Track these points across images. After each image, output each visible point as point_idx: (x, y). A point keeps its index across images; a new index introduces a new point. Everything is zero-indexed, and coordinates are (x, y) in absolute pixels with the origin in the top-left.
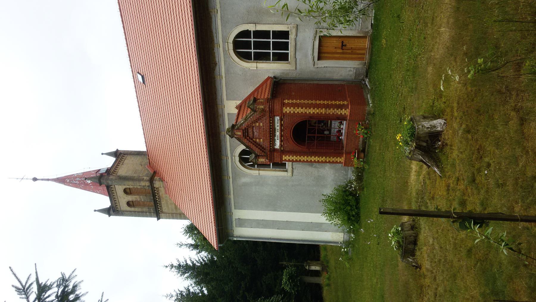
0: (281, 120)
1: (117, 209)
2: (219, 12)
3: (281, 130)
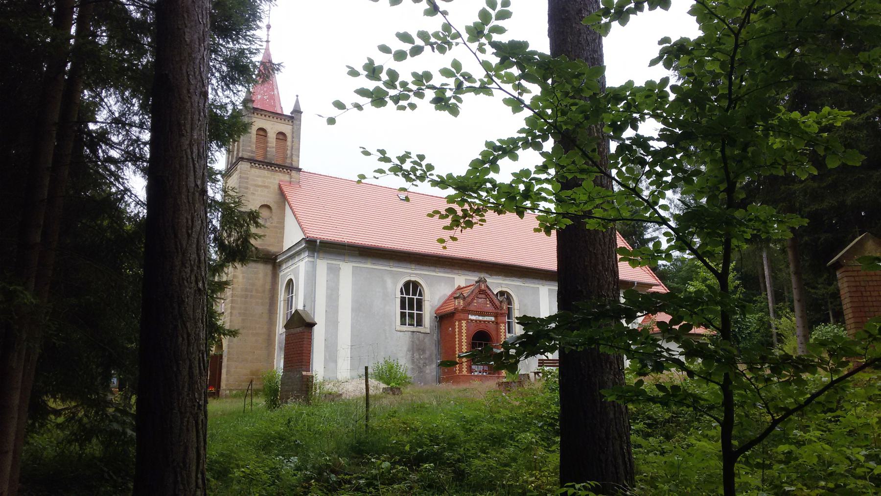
0: (493, 322)
1: (255, 114)
3: (485, 321)
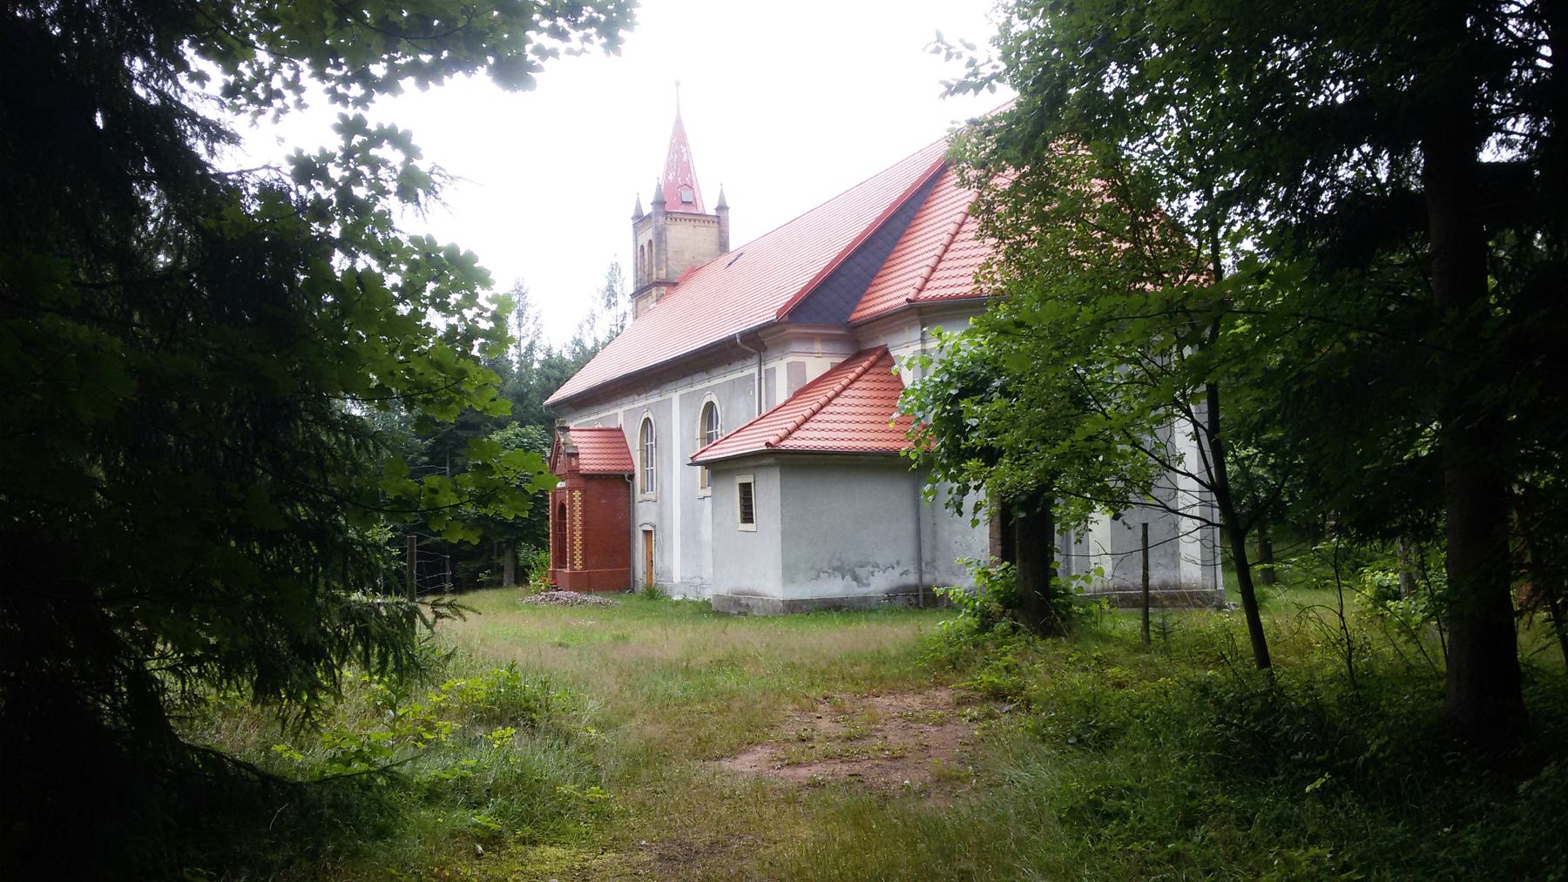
2: (658, 399)
